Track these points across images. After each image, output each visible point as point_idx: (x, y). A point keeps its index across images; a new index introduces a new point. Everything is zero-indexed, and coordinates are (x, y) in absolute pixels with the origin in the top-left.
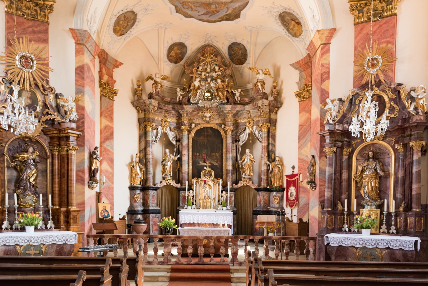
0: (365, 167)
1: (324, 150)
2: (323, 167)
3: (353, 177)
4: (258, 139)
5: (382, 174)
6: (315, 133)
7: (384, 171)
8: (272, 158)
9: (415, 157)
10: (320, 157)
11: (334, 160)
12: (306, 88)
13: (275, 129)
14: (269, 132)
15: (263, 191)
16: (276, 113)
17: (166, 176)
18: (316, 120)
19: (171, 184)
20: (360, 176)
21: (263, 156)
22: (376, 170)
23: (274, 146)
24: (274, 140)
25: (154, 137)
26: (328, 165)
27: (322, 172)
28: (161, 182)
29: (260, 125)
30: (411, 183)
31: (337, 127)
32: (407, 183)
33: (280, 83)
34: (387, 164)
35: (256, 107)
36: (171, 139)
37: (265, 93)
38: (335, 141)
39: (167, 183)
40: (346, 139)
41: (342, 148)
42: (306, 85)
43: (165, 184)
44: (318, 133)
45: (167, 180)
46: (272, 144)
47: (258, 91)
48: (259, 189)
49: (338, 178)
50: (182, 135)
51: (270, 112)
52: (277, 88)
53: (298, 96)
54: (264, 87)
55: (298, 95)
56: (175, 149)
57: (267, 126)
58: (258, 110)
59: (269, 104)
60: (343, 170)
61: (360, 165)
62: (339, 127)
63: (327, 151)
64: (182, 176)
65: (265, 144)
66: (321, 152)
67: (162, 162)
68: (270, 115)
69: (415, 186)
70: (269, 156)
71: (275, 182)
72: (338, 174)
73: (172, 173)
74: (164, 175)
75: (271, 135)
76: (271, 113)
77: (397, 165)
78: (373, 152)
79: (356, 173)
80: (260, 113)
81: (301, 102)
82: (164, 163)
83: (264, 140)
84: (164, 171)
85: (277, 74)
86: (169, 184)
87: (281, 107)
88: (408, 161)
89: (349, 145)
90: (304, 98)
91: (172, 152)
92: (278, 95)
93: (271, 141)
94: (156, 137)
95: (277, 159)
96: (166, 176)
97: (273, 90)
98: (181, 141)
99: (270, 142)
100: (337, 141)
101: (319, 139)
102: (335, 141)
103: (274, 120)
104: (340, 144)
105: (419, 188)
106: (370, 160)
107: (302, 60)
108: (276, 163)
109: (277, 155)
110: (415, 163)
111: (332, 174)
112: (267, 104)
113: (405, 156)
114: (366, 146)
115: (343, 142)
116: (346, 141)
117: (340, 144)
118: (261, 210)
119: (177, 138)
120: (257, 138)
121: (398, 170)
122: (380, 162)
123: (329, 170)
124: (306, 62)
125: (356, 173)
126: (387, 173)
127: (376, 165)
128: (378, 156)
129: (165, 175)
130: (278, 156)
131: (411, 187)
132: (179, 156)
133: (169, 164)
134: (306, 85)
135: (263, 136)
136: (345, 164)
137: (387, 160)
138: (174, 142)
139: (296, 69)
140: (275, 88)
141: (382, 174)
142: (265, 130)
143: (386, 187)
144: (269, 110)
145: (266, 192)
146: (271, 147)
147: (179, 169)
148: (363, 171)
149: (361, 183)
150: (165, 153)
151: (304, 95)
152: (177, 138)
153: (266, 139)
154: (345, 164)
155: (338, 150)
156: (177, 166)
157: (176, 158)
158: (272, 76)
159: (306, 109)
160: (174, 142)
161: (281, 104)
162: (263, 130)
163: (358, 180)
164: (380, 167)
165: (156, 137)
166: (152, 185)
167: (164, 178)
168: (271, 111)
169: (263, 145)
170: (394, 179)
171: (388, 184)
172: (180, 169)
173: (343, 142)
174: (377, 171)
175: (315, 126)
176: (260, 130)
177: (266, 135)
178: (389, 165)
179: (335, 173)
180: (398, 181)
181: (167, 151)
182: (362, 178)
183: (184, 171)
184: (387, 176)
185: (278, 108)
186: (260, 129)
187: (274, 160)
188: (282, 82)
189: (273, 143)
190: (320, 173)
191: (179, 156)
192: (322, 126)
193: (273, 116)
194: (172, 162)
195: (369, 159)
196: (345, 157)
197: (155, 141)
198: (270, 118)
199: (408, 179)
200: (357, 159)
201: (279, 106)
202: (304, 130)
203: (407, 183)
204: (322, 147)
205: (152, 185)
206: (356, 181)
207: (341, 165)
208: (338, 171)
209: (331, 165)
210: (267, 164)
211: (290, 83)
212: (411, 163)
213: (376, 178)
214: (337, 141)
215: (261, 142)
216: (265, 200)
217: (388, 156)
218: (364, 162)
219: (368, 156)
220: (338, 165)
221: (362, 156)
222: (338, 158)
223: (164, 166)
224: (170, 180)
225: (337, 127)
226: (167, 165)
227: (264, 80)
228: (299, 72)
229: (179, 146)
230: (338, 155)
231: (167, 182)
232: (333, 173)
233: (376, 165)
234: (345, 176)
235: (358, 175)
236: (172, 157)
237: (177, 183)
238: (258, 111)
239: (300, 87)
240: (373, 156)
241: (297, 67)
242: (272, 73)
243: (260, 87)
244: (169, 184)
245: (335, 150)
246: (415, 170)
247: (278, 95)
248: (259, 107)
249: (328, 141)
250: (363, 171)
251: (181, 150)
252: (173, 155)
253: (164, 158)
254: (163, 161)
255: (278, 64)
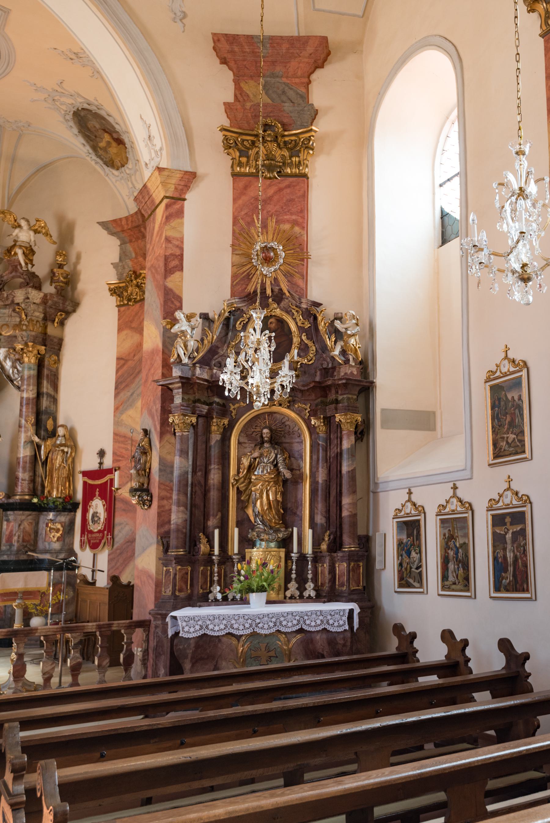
0: (255, 459)
1: (170, 420)
2: (169, 458)
3: (232, 481)
4: (12, 381)
5: (288, 474)
6: (150, 379)
7: (291, 470)
8: (46, 430)
9: (346, 444)
10: (162, 434)
11: (191, 442)
12: (136, 279)
13: (58, 361)
14: (40, 365)
15: (20, 509)
16: (62, 324)
18: (153, 352)
20: (245, 477)
21: (23, 422)
22: (276, 466)
23: (55, 400)
24: (55, 386)
26: (177, 453)
27: (166, 467)
29: (19, 346)
30: (340, 494)
31: (198, 371)
32: (333, 493)
33: (73, 259)
34: (296, 455)
35: (9, 302)
37: (33, 275)
38: (195, 402)
40: (217, 400)
41: (208, 417)
42: (135, 272)
44: (157, 381)
46: (48, 395)
47: (16, 266)
48: (8, 504)
49: (199, 483)
51: (45, 319)
52: (65, 268)
53: (115, 293)
54: (31, 261)
55: (115, 291)
57: (35, 352)
58: (14, 310)
59: (45, 300)
60: (210, 464)
61: (245, 455)
62: (201, 373)
63: (177, 421)
65: (29, 393)
66: (164, 423)
68: (46, 327)
69: (346, 501)
70: (38, 424)
71: (52, 488)
72: (199, 474)
75: (46, 375)
76: (50, 325)
77: (315, 457)
78: (271, 430)
79: (238, 472)
80: (18, 320)
81: (122, 309)
83: (28, 385)
85: (66, 237)
87: (74, 311)
88: (334, 451)
89: (224, 411)
90: (129, 300)
92: (67, 283)
93: (46, 387)
95: (61, 431)
97: (55, 270)
99: (45, 390)
100: (199, 401)
101: (159, 394)
102: (195, 402)
103: (55, 340)
104: (204, 409)
105: (354, 504)
106: (266, 445)
107: (127, 218)
108: (58, 442)
109: (61, 421)
110: (345, 456)
111: (187, 473)
112: (38, 301)
113: (328, 440)
114: (257, 417)
115: (210, 404)
116: (218, 404)
117: (204, 409)
118: (13, 558)
120: (8, 377)
121: (318, 469)
122: (283, 450)
123: (180, 464)
124: (135, 224)
125: (238, 472)
126: (298, 472)
127: (276, 457)
128: (279, 438)
130: (62, 426)
131: (341, 502)
134: (135, 272)
135: (26, 373)
136: (215, 452)
137: (296, 447)
139: (112, 234)
140: (61, 266)
141: (288, 474)
142: (30, 360)
143: (296, 501)
144: (42, 316)
145: (27, 513)
146: (45, 403)
148: (251, 468)
149: (247, 492)
151: (128, 293)
153: (33, 381)
154: (215, 452)
155: (201, 420)
158: (55, 238)
159: (134, 325)
161: (76, 305)
162: (26, 360)
163: (242, 487)
164: (284, 460)
168: (47, 318)
169: (25, 395)
170: (311, 485)
171: (299, 496)
173: (210, 404)
174: (278, 470)
175: (152, 365)
176: (18, 360)
177: (34, 372)
178: (301, 457)
179: (194, 472)
180: (317, 490)
182: (250, 482)
184: (298, 479)
185: (68, 314)
186: (17, 357)
187: (53, 434)
188: (79, 257)
189: (51, 391)
190: (160, 470)
192: (167, 366)
193: (52, 330)
195: (262, 443)
196: (215, 437)
198: (45, 334)
199: (335, 486)
200: (239, 443)
201: (69, 308)
202: (128, 370)
203: (333, 493)
204: (165, 411)
206: (238, 488)
207: (207, 454)
208: (201, 467)
209: (183, 453)
210: (32, 442)
211: (98, 263)
212: (339, 455)
213: (276, 483)
214: (199, 401)
215: (18, 388)
216: (24, 531)
217: (297, 440)
218: (254, 450)
219: (262, 437)
220: (201, 453)
221: (250, 437)
222: (200, 439)
225: (198, 371)
227: (32, 244)
228: (118, 243)
230: (201, 431)
232: (190, 470)
233: (276, 457)
234: (215, 477)
235: (241, 475)
238: (13, 314)
239: (122, 274)
240: (271, 437)
241: (115, 230)
242: (54, 231)
243: (21, 258)
245: (194, 420)
246: (345, 469)
247: (67, 283)
248: (18, 304)
249: (178, 400)
250: (251, 468)
255: (70, 216)
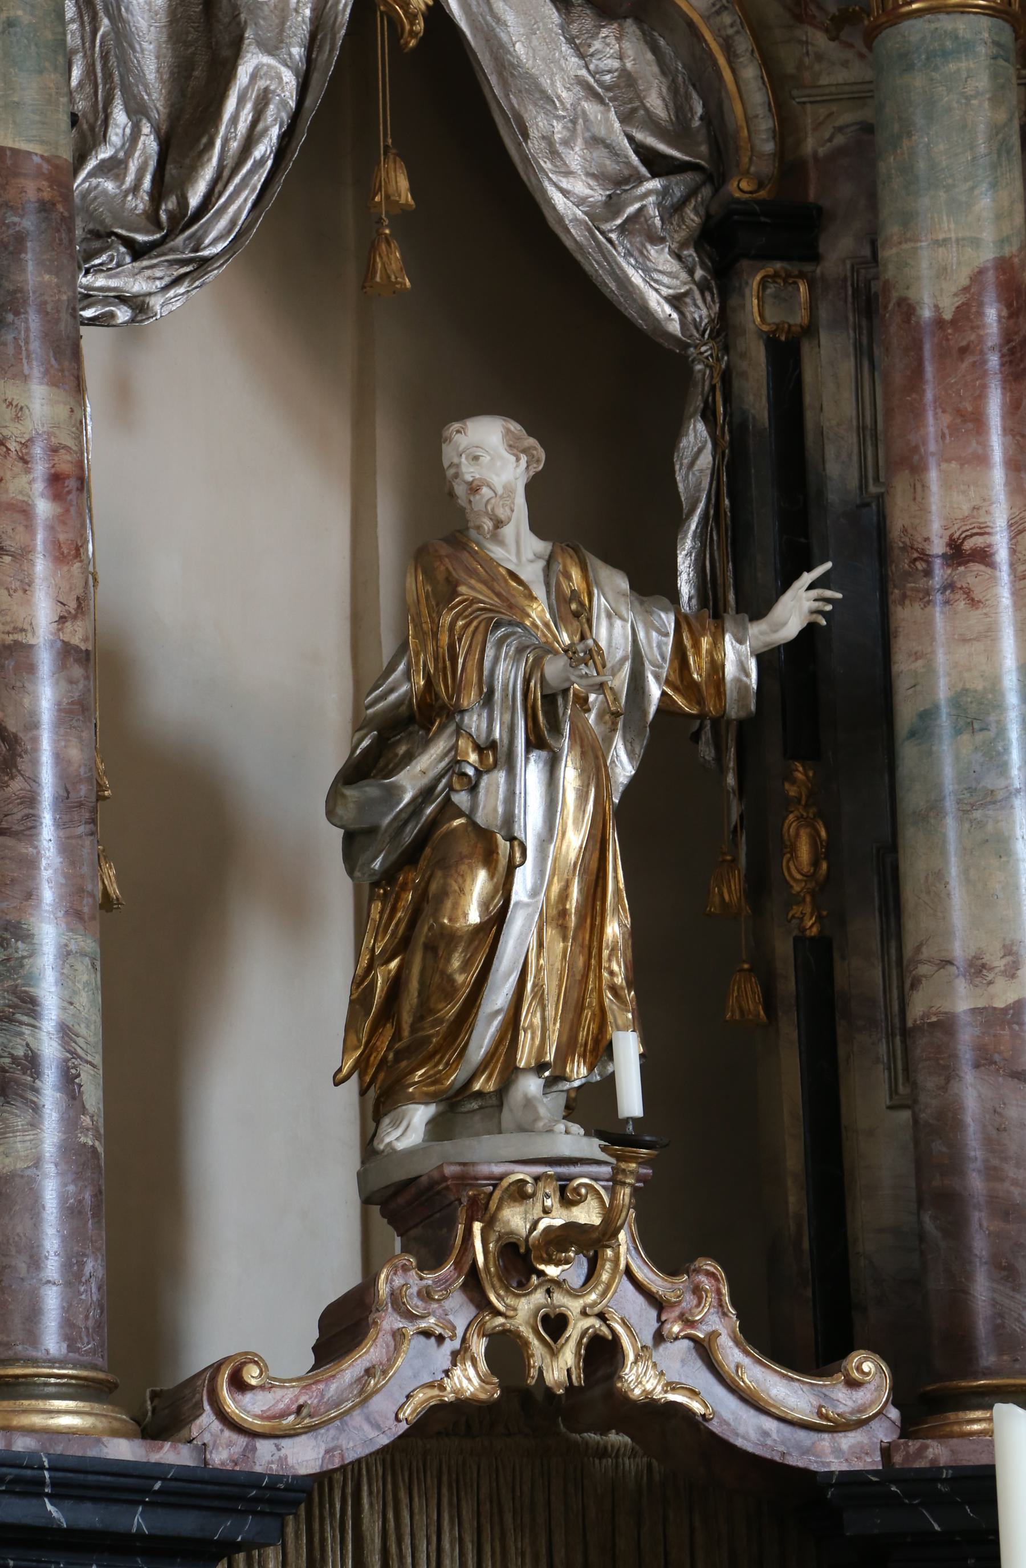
17: (490, 1154)
19: (639, 1381)
25: (131, 141)
28: (342, 1329)
36: (569, 192)
39: (506, 1353)
43: (469, 1381)
45: (519, 1262)
50: (862, 95)
56: (696, 454)
64: (934, 1142)
67: (358, 771)
73: (628, 1049)
74: (411, 1128)
82: (409, 781)
84: (407, 1028)
86: (559, 1367)
91: (608, 515)
94: (187, 129)
96: (490, 1154)
98: (839, 250)
119: (715, 173)
129: (456, 1110)
132: (795, 609)
133: (551, 812)
138: (657, 284)
147: (819, 956)
150: (443, 530)
152: (715, 173)
156: (761, 883)
157: (738, 658)
160: (657, 284)
165: (187, 129)
166: (67, 1416)
167: (414, 1213)
172: (860, 971)
181: (494, 458)
183: (963, 1000)
191: (795, 609)
194: (623, 767)
197: (167, 228)
205: (67, 1416)
223: (411, 862)
224: (590, 1243)
226: (494, 847)
229: (786, 354)
231: (523, 1310)
236: (623, 629)
237: (812, 1349)
244: (559, 1367)
251: (838, 467)
252: (652, 583)
253: (402, 687)
254: (386, 738)
